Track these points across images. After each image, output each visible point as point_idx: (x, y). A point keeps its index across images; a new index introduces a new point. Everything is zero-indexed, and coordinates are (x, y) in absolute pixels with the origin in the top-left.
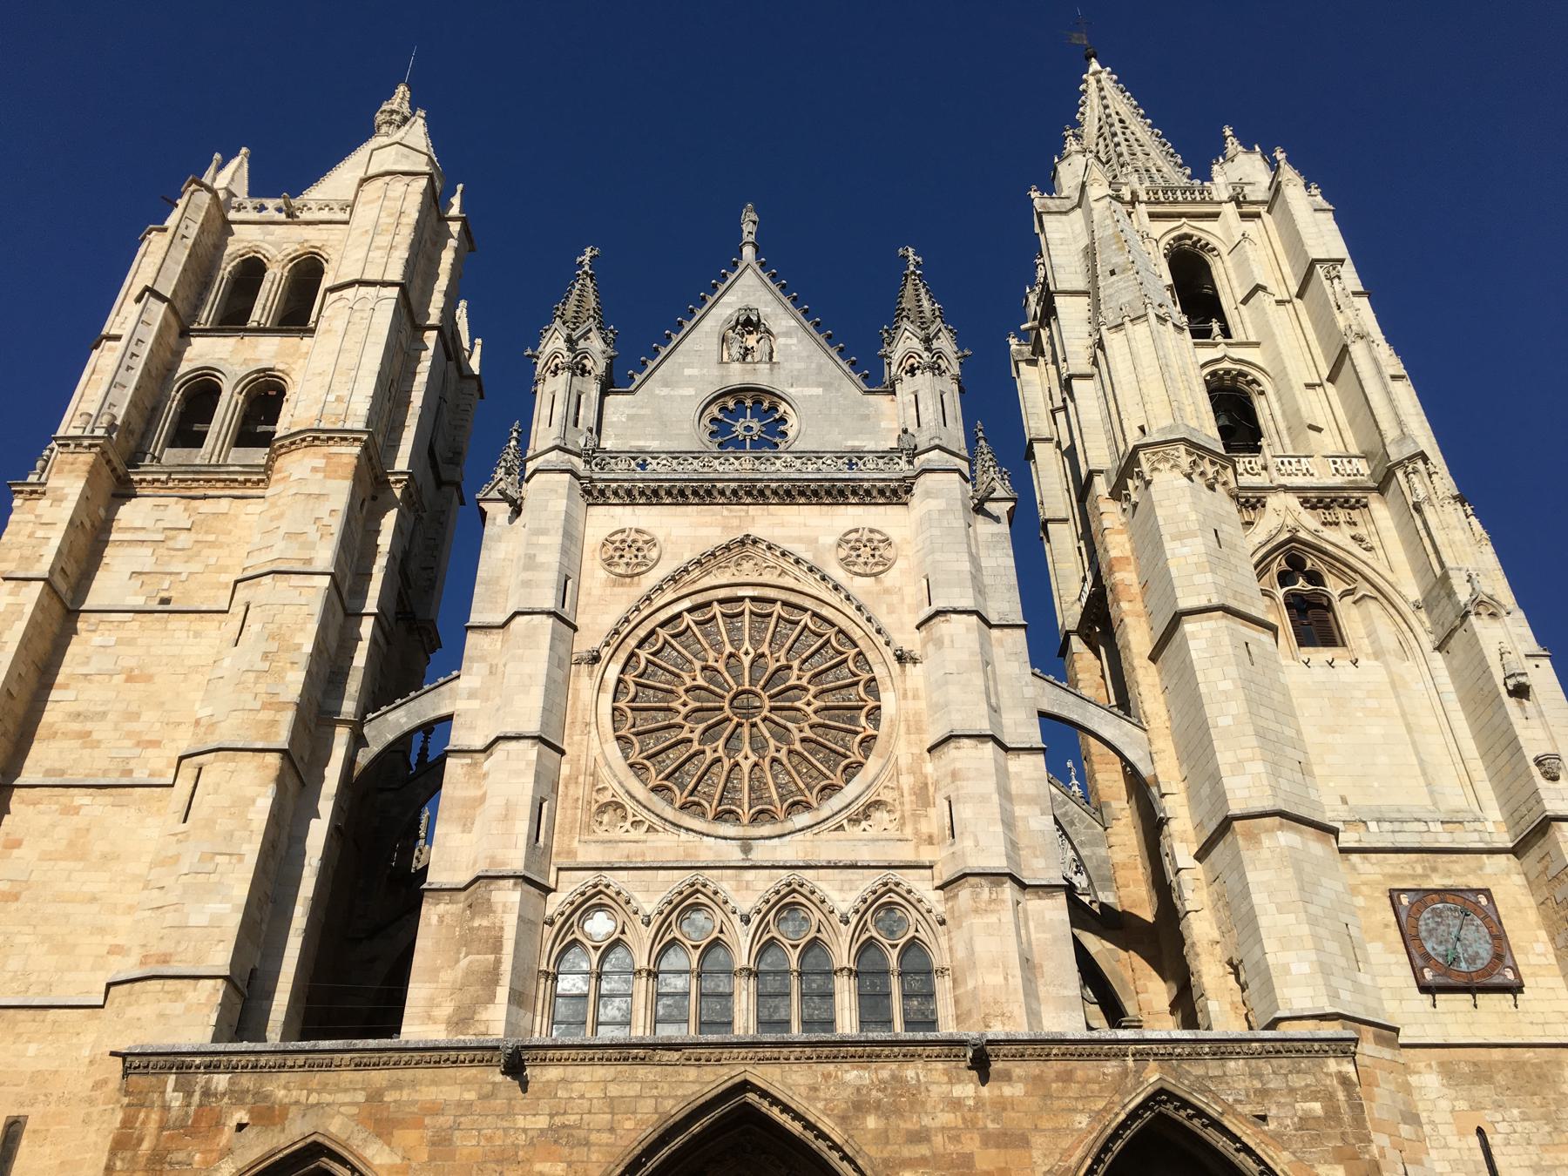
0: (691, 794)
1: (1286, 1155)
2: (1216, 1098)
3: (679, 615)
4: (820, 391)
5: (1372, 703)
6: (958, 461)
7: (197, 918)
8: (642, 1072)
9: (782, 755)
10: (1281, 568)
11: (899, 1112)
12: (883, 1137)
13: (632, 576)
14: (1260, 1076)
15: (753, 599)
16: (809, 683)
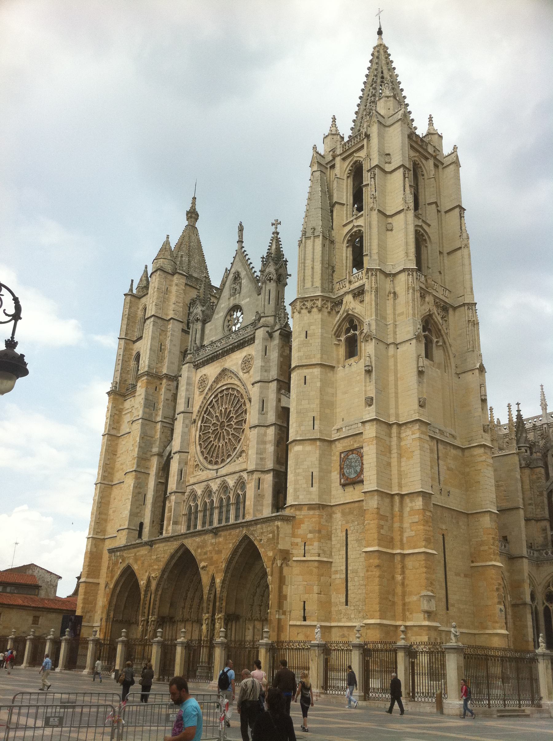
0: (212, 457)
1: (263, 550)
2: (254, 536)
3: (212, 401)
4: (248, 300)
5: (358, 378)
6: (269, 318)
7: (124, 516)
8: (169, 543)
9: (227, 441)
10: (346, 327)
11: (202, 547)
12: (200, 554)
13: (203, 391)
14: (262, 528)
15: (226, 389)
16: (235, 414)
